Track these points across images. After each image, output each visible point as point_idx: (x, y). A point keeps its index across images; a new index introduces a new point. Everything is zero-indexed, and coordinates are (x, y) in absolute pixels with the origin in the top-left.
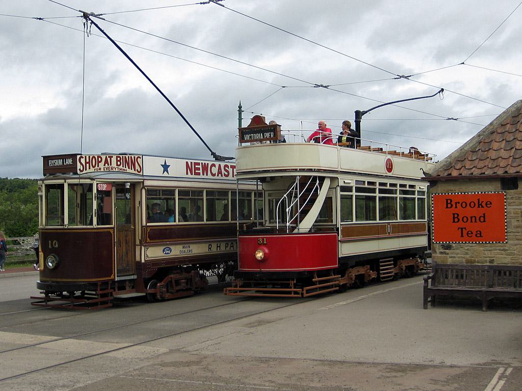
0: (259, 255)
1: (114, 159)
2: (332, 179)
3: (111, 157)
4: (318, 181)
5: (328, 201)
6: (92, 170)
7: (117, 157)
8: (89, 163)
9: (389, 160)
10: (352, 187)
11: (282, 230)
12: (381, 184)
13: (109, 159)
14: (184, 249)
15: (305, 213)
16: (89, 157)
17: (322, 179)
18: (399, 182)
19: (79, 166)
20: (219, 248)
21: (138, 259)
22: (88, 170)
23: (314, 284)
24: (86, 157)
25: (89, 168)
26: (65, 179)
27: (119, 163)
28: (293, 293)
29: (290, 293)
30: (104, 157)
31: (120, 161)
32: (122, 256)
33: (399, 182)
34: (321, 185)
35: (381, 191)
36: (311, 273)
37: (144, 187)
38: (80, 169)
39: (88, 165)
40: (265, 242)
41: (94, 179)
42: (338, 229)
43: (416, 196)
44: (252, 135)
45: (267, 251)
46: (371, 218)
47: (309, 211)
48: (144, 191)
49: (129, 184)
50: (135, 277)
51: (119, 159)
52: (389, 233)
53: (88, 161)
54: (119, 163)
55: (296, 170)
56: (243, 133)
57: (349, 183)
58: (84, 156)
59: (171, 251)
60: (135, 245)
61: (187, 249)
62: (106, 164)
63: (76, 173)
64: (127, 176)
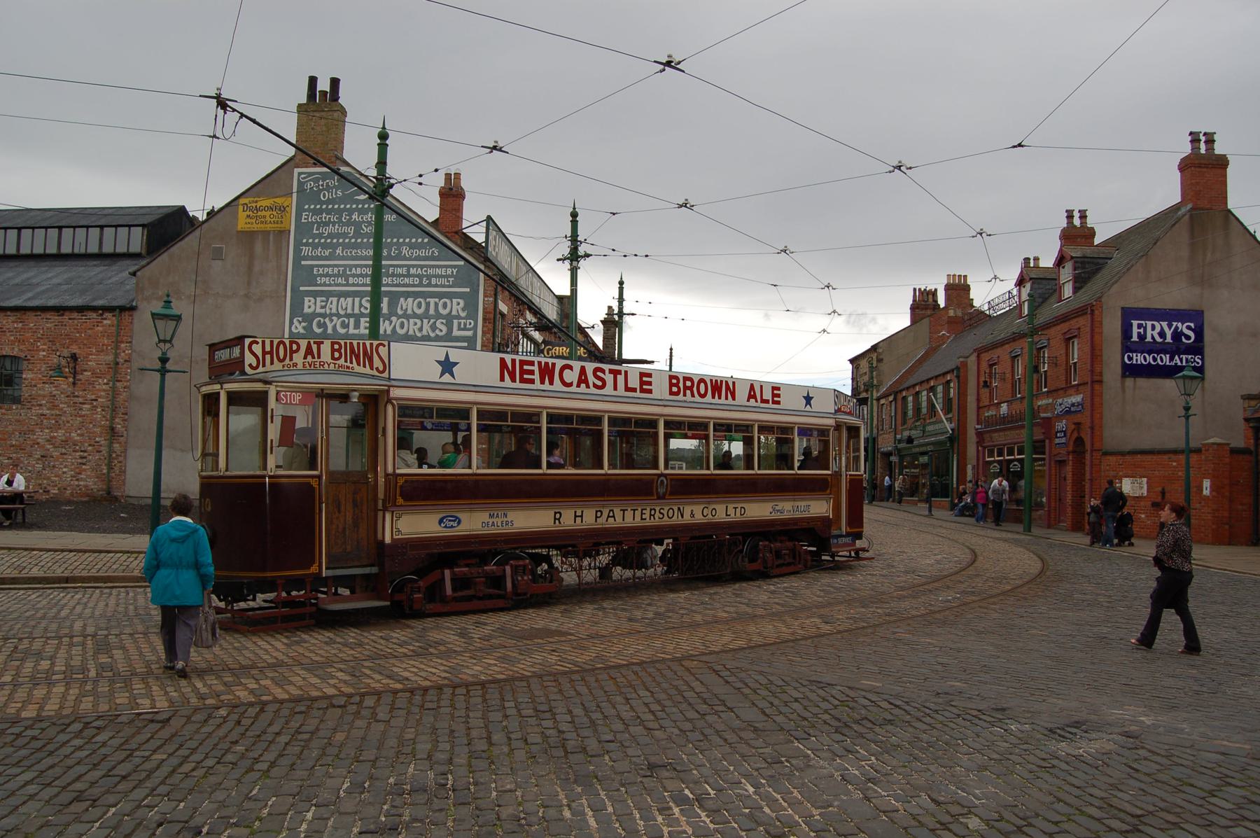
1: (326, 347)
3: (319, 344)
6: (277, 365)
7: (333, 344)
8: (271, 353)
13: (315, 347)
14: (491, 521)
16: (272, 342)
19: (249, 359)
20: (579, 519)
21: (380, 536)
22: (268, 367)
24: (263, 342)
25: (272, 363)
26: (221, 384)
27: (337, 355)
30: (304, 344)
31: (339, 351)
32: (344, 529)
37: (389, 401)
38: (250, 365)
39: (268, 357)
41: (269, 383)
48: (390, 408)
49: (356, 394)
50: (374, 570)
51: (336, 347)
53: (268, 348)
54: (337, 355)
58: (260, 341)
59: (459, 523)
60: (376, 510)
61: (499, 521)
62: (309, 357)
63: (243, 373)
64: (359, 378)
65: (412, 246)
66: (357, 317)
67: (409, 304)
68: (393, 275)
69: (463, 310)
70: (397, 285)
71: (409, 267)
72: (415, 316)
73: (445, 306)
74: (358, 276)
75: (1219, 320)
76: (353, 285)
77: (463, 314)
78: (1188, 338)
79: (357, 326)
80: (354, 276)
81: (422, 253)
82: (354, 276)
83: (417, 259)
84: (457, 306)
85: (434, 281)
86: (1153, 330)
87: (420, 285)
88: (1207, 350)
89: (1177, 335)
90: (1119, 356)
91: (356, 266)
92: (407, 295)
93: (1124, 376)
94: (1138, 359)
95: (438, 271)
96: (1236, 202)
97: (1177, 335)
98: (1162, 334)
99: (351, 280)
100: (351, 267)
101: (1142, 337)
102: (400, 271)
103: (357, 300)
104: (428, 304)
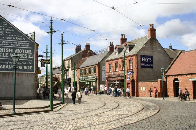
65: (18, 37)
66: (5, 53)
67: (18, 51)
68: (14, 44)
69: (31, 52)
70: (15, 46)
71: (18, 42)
72: (19, 53)
73: (27, 51)
74: (5, 43)
75: (155, 58)
76: (4, 45)
77: (31, 53)
78: (151, 61)
79: (5, 55)
80: (4, 43)
81: (21, 39)
82: (4, 43)
83: (20, 40)
84: (29, 52)
85: (24, 46)
86: (146, 59)
87: (21, 46)
88: (153, 63)
89: (149, 60)
90: (140, 64)
91: (4, 41)
92: (17, 48)
93: (141, 68)
94: (143, 64)
95: (25, 43)
96: (157, 37)
97: (149, 60)
98: (147, 60)
99: (3, 44)
100: (3, 41)
101: (144, 60)
102: (15, 43)
103: (5, 49)
104: (23, 51)
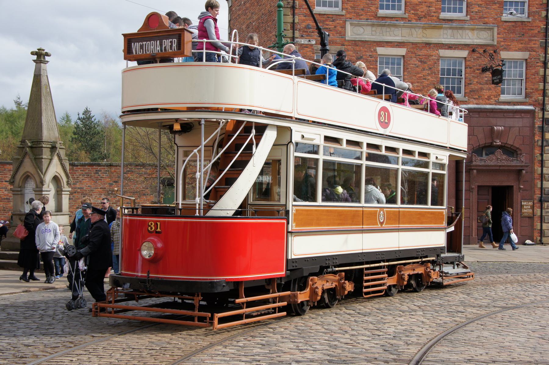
0: (146, 252)
2: (279, 129)
4: (254, 131)
5: (272, 166)
9: (384, 109)
10: (318, 146)
11: (189, 211)
12: (369, 146)
15: (229, 181)
17: (261, 129)
18: (402, 146)
23: (240, 306)
28: (196, 319)
29: (191, 318)
33: (402, 146)
34: (259, 137)
35: (370, 157)
36: (237, 283)
40: (159, 230)
42: (287, 212)
43: (431, 170)
44: (144, 43)
45: (160, 245)
46: (354, 199)
47: (235, 179)
52: (382, 223)
55: (218, 110)
56: (129, 39)
57: (312, 140)
